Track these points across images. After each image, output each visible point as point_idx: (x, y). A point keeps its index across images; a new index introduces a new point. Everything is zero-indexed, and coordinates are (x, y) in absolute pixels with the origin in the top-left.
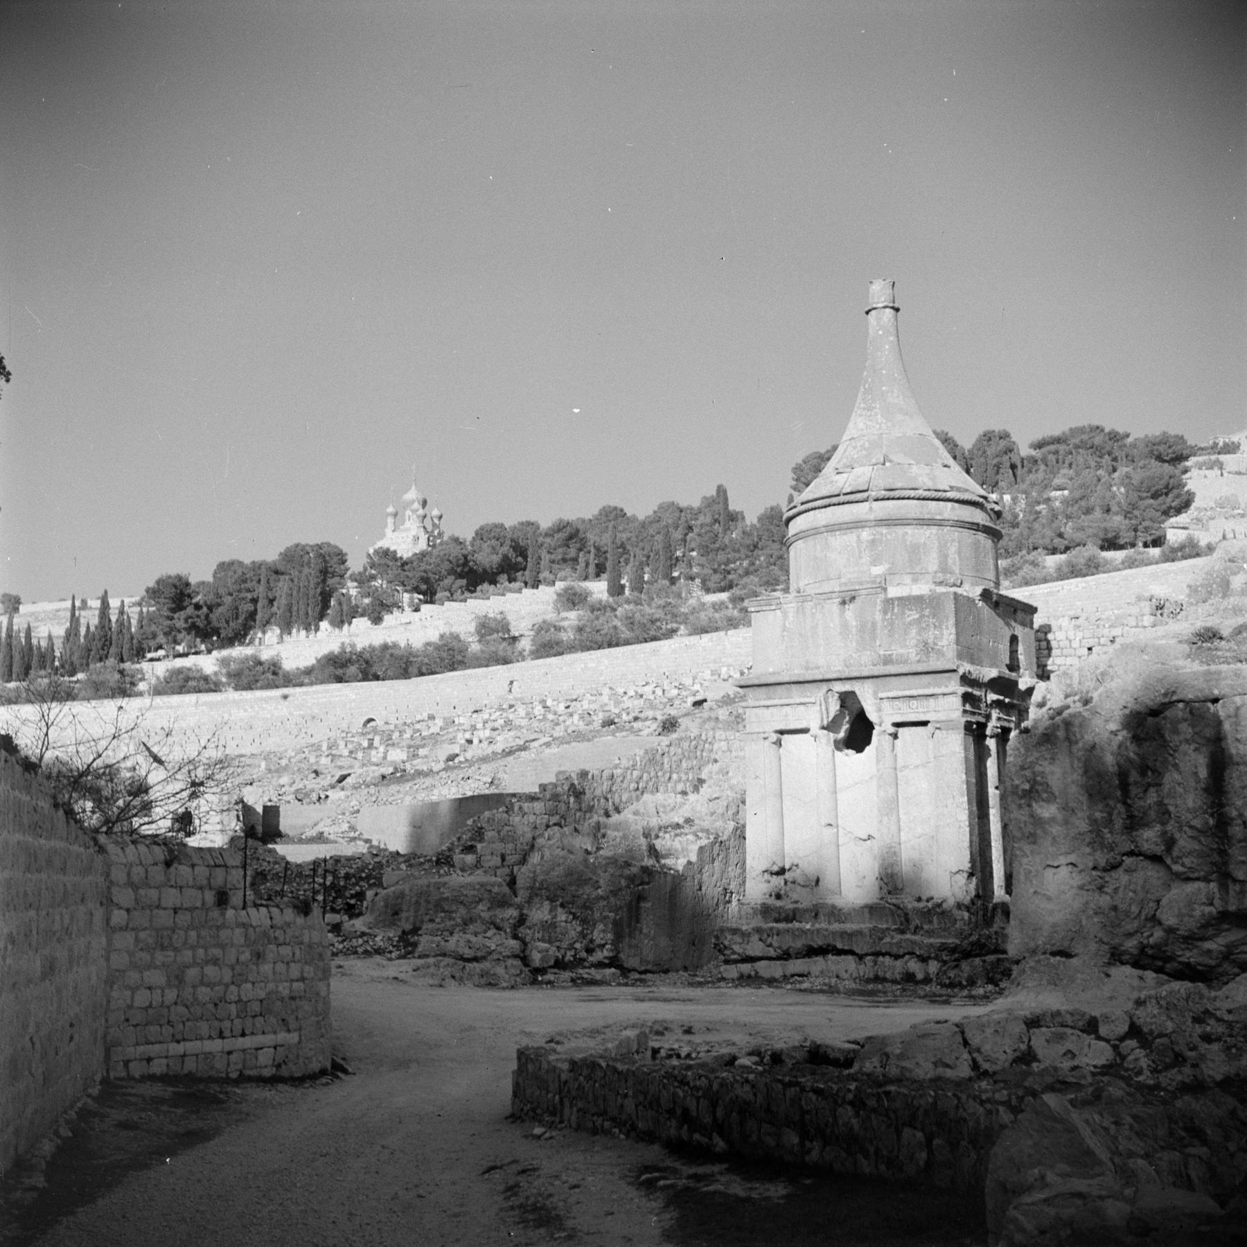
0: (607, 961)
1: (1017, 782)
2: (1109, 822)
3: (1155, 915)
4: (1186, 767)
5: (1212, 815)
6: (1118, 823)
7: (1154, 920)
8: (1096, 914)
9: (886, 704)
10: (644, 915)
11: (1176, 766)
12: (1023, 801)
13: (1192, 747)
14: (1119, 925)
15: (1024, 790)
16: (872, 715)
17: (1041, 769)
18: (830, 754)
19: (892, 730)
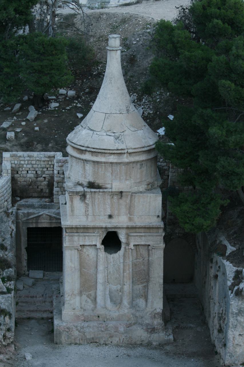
1: (234, 311)
12: (234, 316)
15: (236, 313)
19: (132, 247)
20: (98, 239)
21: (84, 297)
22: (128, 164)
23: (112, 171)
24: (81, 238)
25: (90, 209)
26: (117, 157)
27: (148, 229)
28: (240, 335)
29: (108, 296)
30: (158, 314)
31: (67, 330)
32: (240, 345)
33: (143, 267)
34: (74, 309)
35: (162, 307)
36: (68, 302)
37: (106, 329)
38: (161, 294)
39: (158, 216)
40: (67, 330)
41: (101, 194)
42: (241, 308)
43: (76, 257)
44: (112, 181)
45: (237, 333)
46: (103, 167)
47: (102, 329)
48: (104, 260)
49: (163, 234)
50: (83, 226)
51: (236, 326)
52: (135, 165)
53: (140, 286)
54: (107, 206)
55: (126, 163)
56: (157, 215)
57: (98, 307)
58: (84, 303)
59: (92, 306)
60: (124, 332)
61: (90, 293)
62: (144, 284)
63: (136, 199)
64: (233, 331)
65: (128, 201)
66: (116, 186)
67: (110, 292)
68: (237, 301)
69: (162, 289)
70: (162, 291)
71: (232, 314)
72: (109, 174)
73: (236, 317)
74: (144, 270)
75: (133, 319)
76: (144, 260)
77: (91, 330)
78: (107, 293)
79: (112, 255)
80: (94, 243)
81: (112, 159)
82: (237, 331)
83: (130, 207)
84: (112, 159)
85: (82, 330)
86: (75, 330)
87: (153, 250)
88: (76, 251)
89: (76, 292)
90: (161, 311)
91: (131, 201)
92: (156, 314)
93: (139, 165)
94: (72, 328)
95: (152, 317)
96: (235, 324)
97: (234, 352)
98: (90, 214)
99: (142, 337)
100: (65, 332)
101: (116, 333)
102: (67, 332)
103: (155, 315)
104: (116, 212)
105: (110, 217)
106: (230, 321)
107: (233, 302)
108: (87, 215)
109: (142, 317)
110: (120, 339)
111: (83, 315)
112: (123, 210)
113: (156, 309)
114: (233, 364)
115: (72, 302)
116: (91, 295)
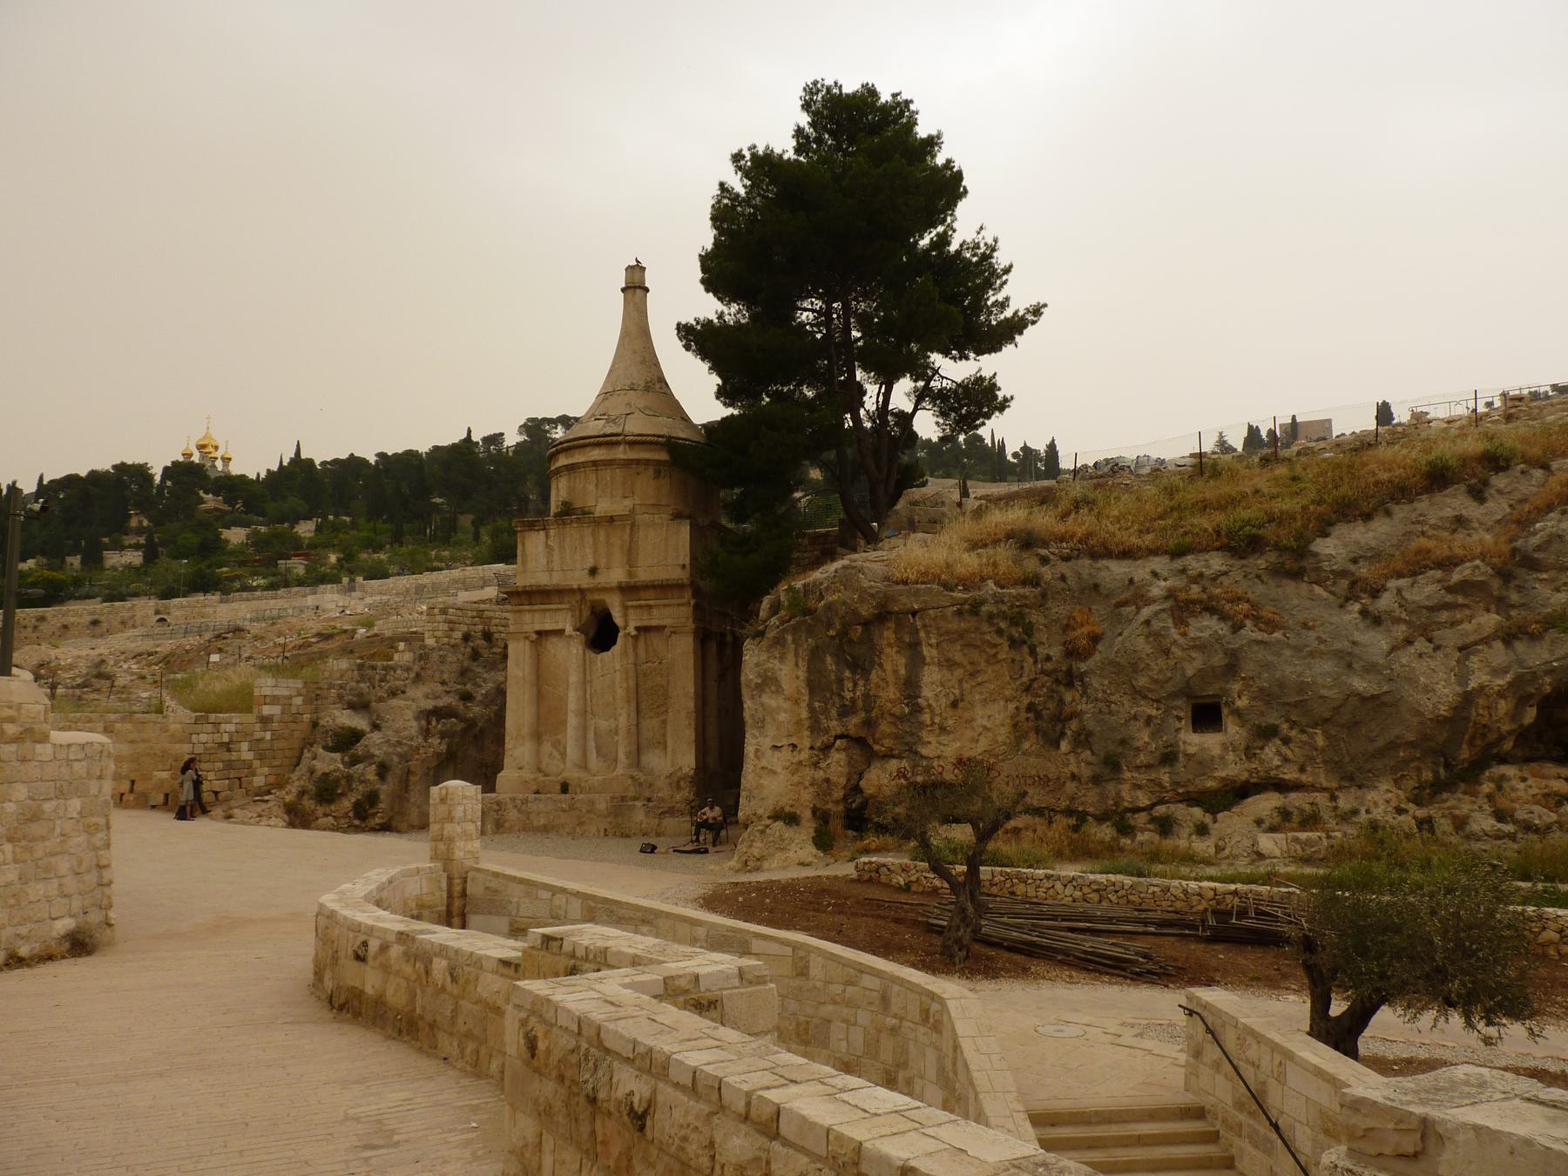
0: (377, 827)
1: (751, 677)
2: (826, 712)
3: (858, 785)
4: (888, 667)
5: (907, 705)
6: (834, 712)
7: (857, 789)
8: (812, 784)
9: (631, 611)
10: (412, 787)
11: (881, 665)
13: (895, 649)
14: (830, 795)
15: (757, 683)
16: (618, 619)
17: (771, 665)
18: (581, 652)
19: (634, 633)
20: (569, 617)
21: (547, 747)
22: (628, 463)
23: (597, 478)
24: (537, 616)
25: (556, 557)
26: (605, 451)
27: (663, 588)
28: (775, 747)
29: (592, 745)
30: (684, 777)
31: (496, 807)
32: (774, 772)
33: (659, 679)
34: (520, 769)
35: (693, 764)
36: (510, 753)
37: (572, 808)
38: (690, 734)
39: (684, 566)
40: (496, 807)
41: (575, 525)
42: (766, 670)
43: (528, 655)
44: (597, 501)
45: (767, 742)
46: (583, 475)
47: (564, 806)
48: (581, 662)
49: (692, 602)
50: (537, 586)
51: (763, 722)
52: (641, 468)
53: (655, 722)
54: (587, 550)
55: (622, 462)
56: (681, 563)
57: (569, 764)
58: (545, 759)
59: (562, 766)
60: (606, 812)
61: (558, 737)
62: (663, 717)
63: (641, 532)
64: (757, 734)
65: (627, 537)
66: (603, 507)
67: (595, 734)
68: (756, 652)
69: (693, 723)
70: (693, 727)
71: (748, 686)
72: (591, 487)
73: (760, 697)
74: (662, 686)
75: (632, 788)
76: (660, 663)
77: (541, 806)
78: (591, 736)
79: (600, 656)
80: (560, 627)
81: (597, 454)
82: (766, 736)
83: (630, 550)
84: (597, 454)
85: (524, 807)
86: (511, 807)
87: (673, 637)
88: (527, 642)
89: (526, 731)
90: (692, 773)
91: (631, 535)
92: (681, 779)
93: (651, 471)
94: (506, 805)
95: (670, 784)
96: (760, 715)
97: (757, 788)
98: (555, 569)
99: (643, 826)
100: (492, 813)
101: (592, 816)
102: (497, 811)
103: (678, 782)
104: (602, 563)
105: (593, 571)
106: (745, 706)
107: (747, 657)
108: (551, 571)
109: (651, 785)
110: (598, 831)
111: (535, 780)
112: (618, 557)
113: (680, 768)
114: (754, 819)
115: (517, 753)
116: (559, 743)
